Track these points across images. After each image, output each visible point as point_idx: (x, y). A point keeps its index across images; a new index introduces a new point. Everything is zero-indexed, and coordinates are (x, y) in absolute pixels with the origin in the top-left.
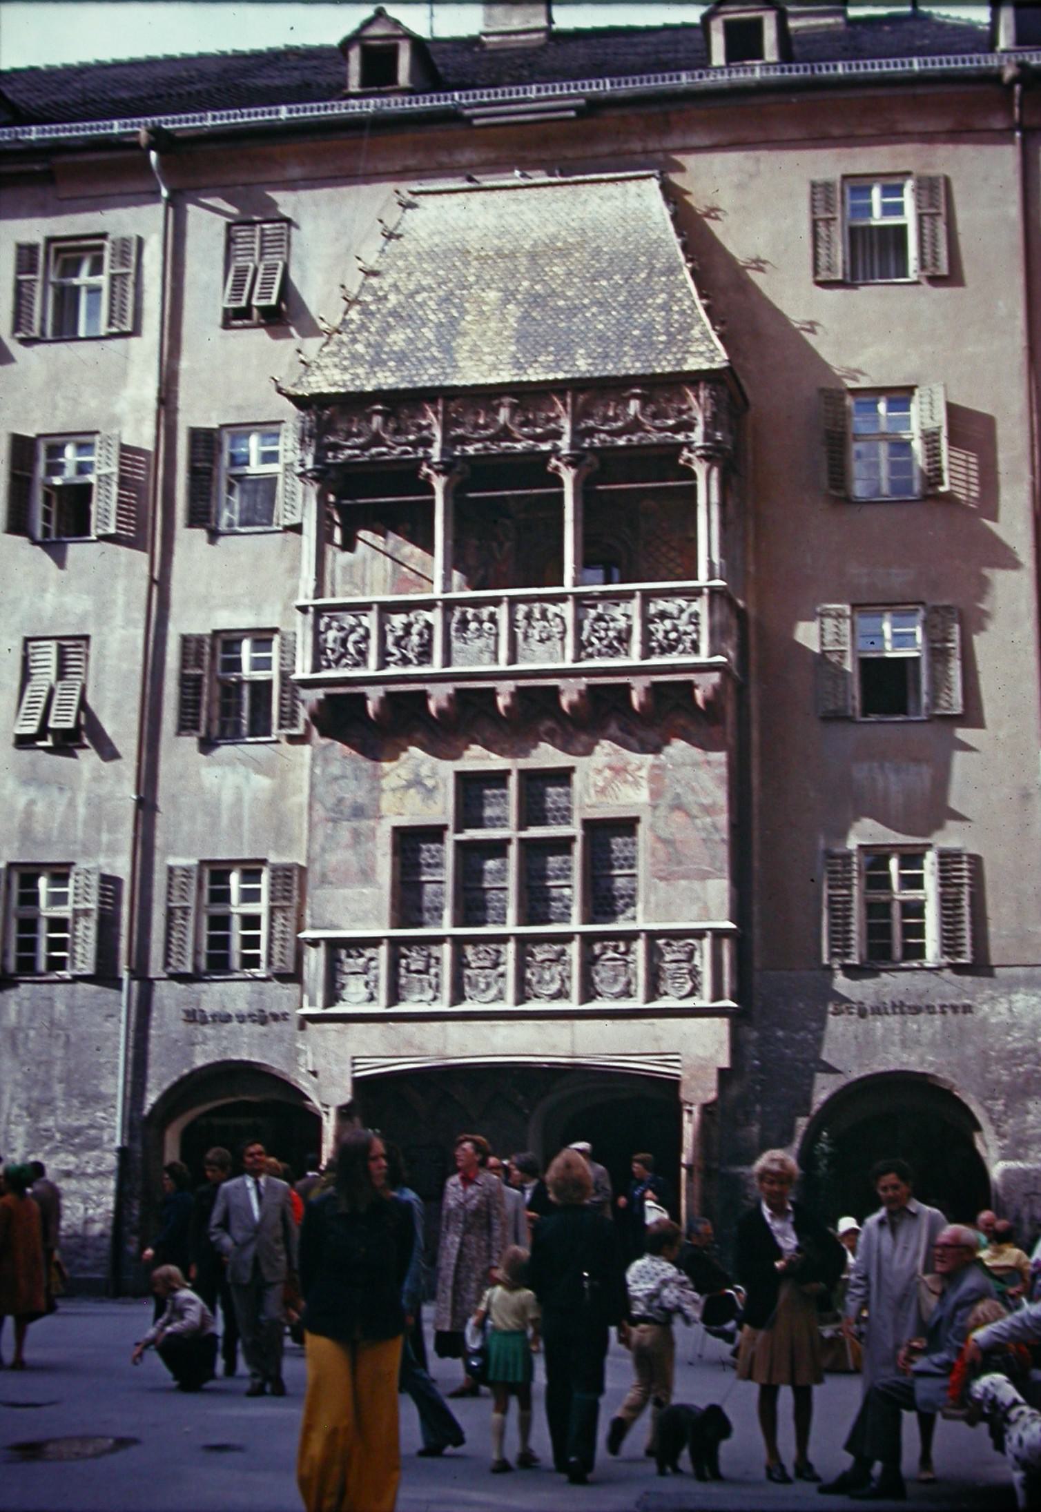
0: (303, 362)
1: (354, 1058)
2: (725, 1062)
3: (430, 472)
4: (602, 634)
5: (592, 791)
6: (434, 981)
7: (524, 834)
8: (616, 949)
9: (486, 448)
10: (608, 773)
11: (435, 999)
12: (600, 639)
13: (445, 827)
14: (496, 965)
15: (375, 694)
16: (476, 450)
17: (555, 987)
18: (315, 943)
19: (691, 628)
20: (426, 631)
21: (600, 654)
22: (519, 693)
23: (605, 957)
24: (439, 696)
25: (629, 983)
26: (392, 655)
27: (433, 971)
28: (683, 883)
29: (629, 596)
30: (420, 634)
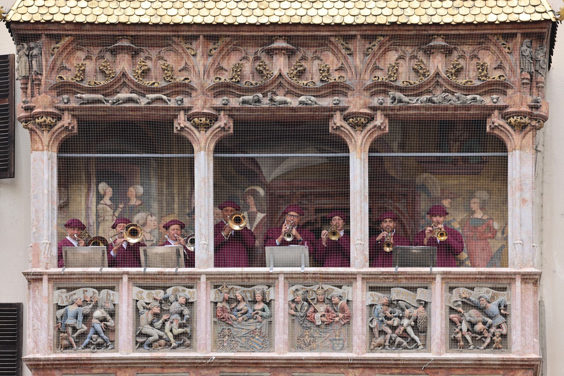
4: (396, 322)
9: (259, 101)
12: (393, 328)
19: (500, 320)
21: (392, 342)
26: (148, 336)
29: (427, 281)
30: (181, 315)
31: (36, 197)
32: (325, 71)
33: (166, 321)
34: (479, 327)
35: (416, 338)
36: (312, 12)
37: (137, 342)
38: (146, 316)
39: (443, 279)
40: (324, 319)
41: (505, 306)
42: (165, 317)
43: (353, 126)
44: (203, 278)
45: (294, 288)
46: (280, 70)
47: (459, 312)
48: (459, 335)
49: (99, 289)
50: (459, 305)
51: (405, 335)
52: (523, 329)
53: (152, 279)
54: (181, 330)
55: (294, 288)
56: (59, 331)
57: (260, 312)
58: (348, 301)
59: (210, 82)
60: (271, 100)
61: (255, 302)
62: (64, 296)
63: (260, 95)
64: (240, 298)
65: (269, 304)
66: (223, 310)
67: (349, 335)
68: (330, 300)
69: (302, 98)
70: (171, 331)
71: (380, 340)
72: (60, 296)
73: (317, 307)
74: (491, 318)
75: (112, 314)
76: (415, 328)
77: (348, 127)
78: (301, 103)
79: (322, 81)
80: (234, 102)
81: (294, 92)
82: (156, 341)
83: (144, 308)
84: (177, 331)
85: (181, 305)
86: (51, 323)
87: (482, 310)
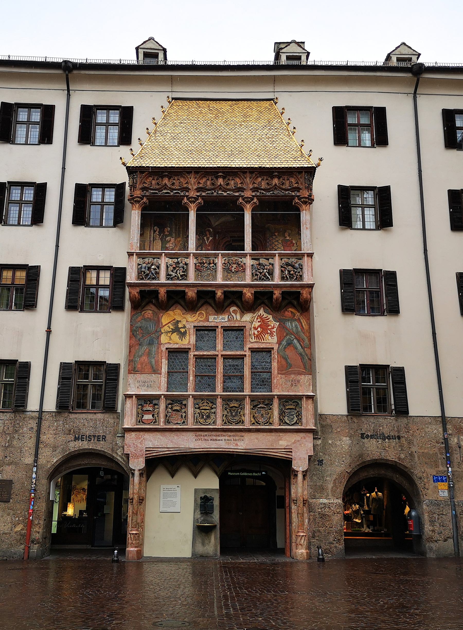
0: (132, 154)
2: (312, 453)
3: (187, 201)
5: (253, 337)
6: (184, 415)
7: (224, 353)
8: (263, 402)
9: (213, 193)
10: (259, 329)
12: (261, 273)
13: (190, 349)
14: (212, 408)
15: (162, 291)
16: (207, 193)
18: (130, 396)
19: (299, 270)
20: (185, 267)
22: (225, 293)
23: (259, 406)
24: (191, 293)
26: (171, 275)
27: (183, 410)
28: (293, 376)
30: (183, 268)
31: (133, 226)
32: (236, 184)
33: (178, 270)
35: (269, 277)
36: (232, 164)
37: (167, 278)
39: (278, 255)
40: (235, 270)
41: (301, 265)
42: (177, 269)
44: (192, 255)
45: (224, 259)
46: (220, 183)
48: (285, 275)
49: (154, 258)
50: (284, 265)
51: (265, 275)
52: (308, 273)
53: (173, 255)
54: (183, 273)
55: (224, 259)
56: (139, 273)
57: (212, 267)
58: (244, 263)
59: (195, 187)
60: (217, 193)
61: (210, 264)
62: (141, 260)
63: (213, 191)
64: (205, 262)
65: (215, 264)
67: (245, 276)
68: (238, 263)
70: (179, 274)
72: (140, 261)
73: (233, 265)
75: (158, 267)
77: (244, 202)
78: (227, 194)
79: (235, 187)
80: (204, 194)
82: (174, 277)
83: (170, 265)
84: (182, 274)
85: (183, 264)
86: (136, 270)
87: (293, 266)
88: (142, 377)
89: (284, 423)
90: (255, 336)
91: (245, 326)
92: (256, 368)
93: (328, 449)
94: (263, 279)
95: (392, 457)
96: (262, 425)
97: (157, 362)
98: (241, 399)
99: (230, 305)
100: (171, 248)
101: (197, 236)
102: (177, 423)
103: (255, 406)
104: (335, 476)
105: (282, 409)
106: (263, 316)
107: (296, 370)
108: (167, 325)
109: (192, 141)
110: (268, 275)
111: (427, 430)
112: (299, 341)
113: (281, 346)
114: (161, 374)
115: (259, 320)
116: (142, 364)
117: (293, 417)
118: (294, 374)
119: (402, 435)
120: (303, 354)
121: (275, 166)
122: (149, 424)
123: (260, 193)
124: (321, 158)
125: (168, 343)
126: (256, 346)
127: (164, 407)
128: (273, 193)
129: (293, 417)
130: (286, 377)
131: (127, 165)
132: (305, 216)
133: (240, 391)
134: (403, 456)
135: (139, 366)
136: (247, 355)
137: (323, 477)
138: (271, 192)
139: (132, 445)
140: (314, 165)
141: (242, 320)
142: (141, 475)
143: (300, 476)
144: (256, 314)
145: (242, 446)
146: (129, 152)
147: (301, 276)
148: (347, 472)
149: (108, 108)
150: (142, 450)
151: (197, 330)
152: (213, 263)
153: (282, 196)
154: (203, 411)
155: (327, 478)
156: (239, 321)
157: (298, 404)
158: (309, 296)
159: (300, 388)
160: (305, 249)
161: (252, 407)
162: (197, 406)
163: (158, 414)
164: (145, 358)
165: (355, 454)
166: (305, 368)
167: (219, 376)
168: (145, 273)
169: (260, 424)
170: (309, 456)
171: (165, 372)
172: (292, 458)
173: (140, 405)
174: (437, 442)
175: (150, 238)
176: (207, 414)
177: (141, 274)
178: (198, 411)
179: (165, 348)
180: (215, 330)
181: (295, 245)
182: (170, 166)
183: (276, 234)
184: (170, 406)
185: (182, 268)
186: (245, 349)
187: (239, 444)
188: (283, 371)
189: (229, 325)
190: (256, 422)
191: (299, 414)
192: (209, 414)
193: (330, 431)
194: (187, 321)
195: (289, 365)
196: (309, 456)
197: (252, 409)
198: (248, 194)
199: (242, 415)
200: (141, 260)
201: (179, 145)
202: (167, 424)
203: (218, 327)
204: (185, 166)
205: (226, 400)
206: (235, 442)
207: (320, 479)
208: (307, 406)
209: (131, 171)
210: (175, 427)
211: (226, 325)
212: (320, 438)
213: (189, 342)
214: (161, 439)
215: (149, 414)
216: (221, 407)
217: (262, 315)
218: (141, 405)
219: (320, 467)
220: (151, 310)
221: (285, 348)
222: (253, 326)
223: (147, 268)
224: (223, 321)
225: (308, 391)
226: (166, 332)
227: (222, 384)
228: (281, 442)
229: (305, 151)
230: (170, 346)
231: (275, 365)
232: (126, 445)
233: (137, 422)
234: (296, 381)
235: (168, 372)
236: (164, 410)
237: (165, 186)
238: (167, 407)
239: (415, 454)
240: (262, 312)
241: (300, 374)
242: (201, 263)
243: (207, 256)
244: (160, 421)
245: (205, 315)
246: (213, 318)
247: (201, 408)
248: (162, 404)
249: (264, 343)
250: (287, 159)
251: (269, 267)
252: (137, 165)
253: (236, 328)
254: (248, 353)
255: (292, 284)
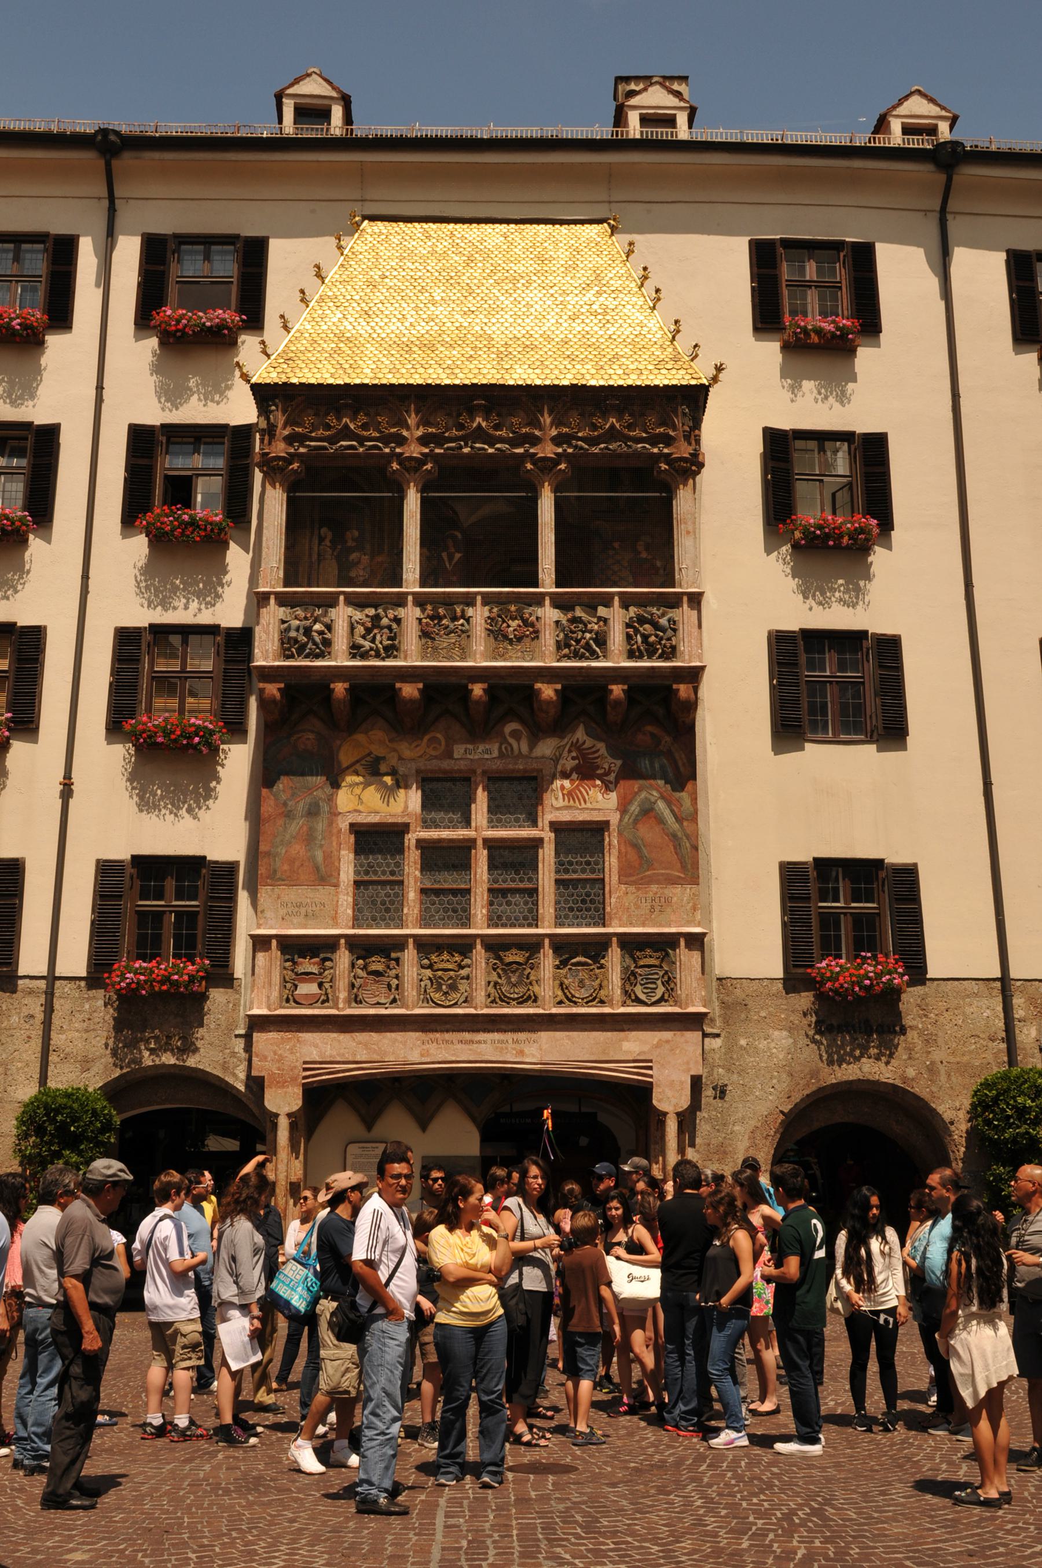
1: (305, 1063)
5: (560, 795)
11: (394, 1001)
12: (578, 641)
14: (462, 967)
16: (449, 448)
17: (521, 990)
19: (670, 633)
20: (394, 626)
24: (409, 690)
25: (601, 986)
26: (360, 647)
28: (654, 888)
29: (606, 601)
30: (389, 628)
34: (652, 639)
35: (597, 649)
38: (360, 630)
41: (675, 622)
42: (376, 631)
43: (542, 471)
44: (410, 598)
47: (634, 627)
56: (283, 643)
60: (472, 447)
61: (454, 619)
65: (468, 620)
66: (427, 624)
69: (498, 446)
71: (566, 651)
73: (510, 622)
74: (664, 631)
75: (329, 627)
76: (596, 641)
78: (497, 449)
80: (437, 451)
81: (491, 441)
82: (367, 652)
84: (387, 643)
85: (390, 620)
86: (276, 635)
87: (656, 626)
88: (291, 894)
89: (633, 1001)
90: (565, 792)
91: (541, 770)
92: (567, 871)
93: (738, 1060)
94: (582, 657)
95: (888, 1075)
96: (582, 1006)
97: (328, 856)
98: (531, 946)
99: (504, 719)
100: (361, 579)
101: (425, 550)
102: (378, 1003)
103: (564, 963)
104: (753, 1123)
105: (628, 968)
106: (584, 743)
107: (662, 874)
108: (353, 769)
109: (412, 320)
110: (594, 647)
111: (968, 1010)
112: (669, 803)
113: (627, 817)
114: (336, 885)
115: (574, 754)
116: (292, 861)
117: (654, 986)
118: (658, 882)
119: (911, 1024)
120: (679, 834)
121: (611, 383)
122: (310, 1005)
123: (576, 447)
124: (721, 365)
125: (356, 811)
126: (565, 816)
127: (347, 965)
128: (607, 448)
129: (654, 986)
130: (638, 889)
131: (253, 381)
132: (683, 501)
133: (530, 926)
134: (911, 1072)
135: (286, 867)
136: (546, 839)
137: (725, 1125)
138: (602, 446)
139: (270, 1056)
140: (705, 382)
141: (534, 755)
142: (293, 1127)
143: (672, 1127)
144: (566, 740)
145: (533, 1056)
146: (259, 348)
147: (674, 648)
148: (782, 1112)
149: (208, 242)
150: (295, 1067)
151: (424, 780)
152: (463, 617)
153: (627, 456)
154: (440, 973)
155: (736, 1128)
156: (527, 757)
157: (667, 954)
158: (693, 696)
159: (673, 917)
160: (685, 586)
161: (557, 963)
162: (426, 962)
163: (331, 981)
164: (298, 849)
165: (802, 1071)
166: (684, 868)
167: (479, 891)
168: (296, 641)
169: (575, 1003)
170: (692, 1077)
171: (349, 881)
172: (651, 1083)
173: (287, 961)
174: (992, 1040)
175: (310, 555)
176: (450, 982)
177: (289, 645)
178: (428, 973)
179: (347, 823)
180: (468, 780)
181: (661, 572)
182: (358, 381)
183: (616, 545)
184: (361, 962)
185: (386, 630)
186: (540, 824)
187: (526, 1051)
188: (631, 875)
189: (501, 767)
190: (567, 997)
191: (669, 978)
192: (455, 980)
193: (743, 1016)
194: (400, 758)
195: (644, 862)
196: (692, 1077)
197: (558, 967)
198: (548, 450)
199: (534, 983)
200: (288, 610)
201: (380, 331)
202: (354, 1004)
203: (474, 772)
204: (394, 381)
205: (495, 946)
206: (518, 1047)
207: (718, 1131)
208: (687, 959)
209: (264, 394)
210: (372, 1011)
211: (494, 767)
212: (718, 1035)
213: (406, 807)
214: (339, 1041)
215: (311, 981)
216: (483, 965)
217: (581, 741)
218: (292, 960)
219: (719, 1103)
220: (312, 732)
221: (636, 822)
222: (559, 768)
223: (302, 631)
224: (486, 756)
225: (689, 923)
226: (350, 786)
227: (484, 911)
228: (626, 1046)
229: (683, 345)
230: (361, 819)
231: (612, 861)
232: (257, 1056)
233: (281, 1001)
234: (663, 900)
235: (355, 882)
236: (347, 972)
237: (346, 433)
238: (353, 965)
239: (941, 1067)
240: (580, 734)
241: (673, 881)
242: (432, 618)
243: (448, 601)
244: (338, 998)
245: (443, 743)
246: (462, 751)
247: (436, 967)
248: (343, 958)
249: (587, 809)
250: (641, 367)
251: (596, 627)
252: (277, 380)
253: (518, 775)
254: (548, 836)
255: (653, 668)
